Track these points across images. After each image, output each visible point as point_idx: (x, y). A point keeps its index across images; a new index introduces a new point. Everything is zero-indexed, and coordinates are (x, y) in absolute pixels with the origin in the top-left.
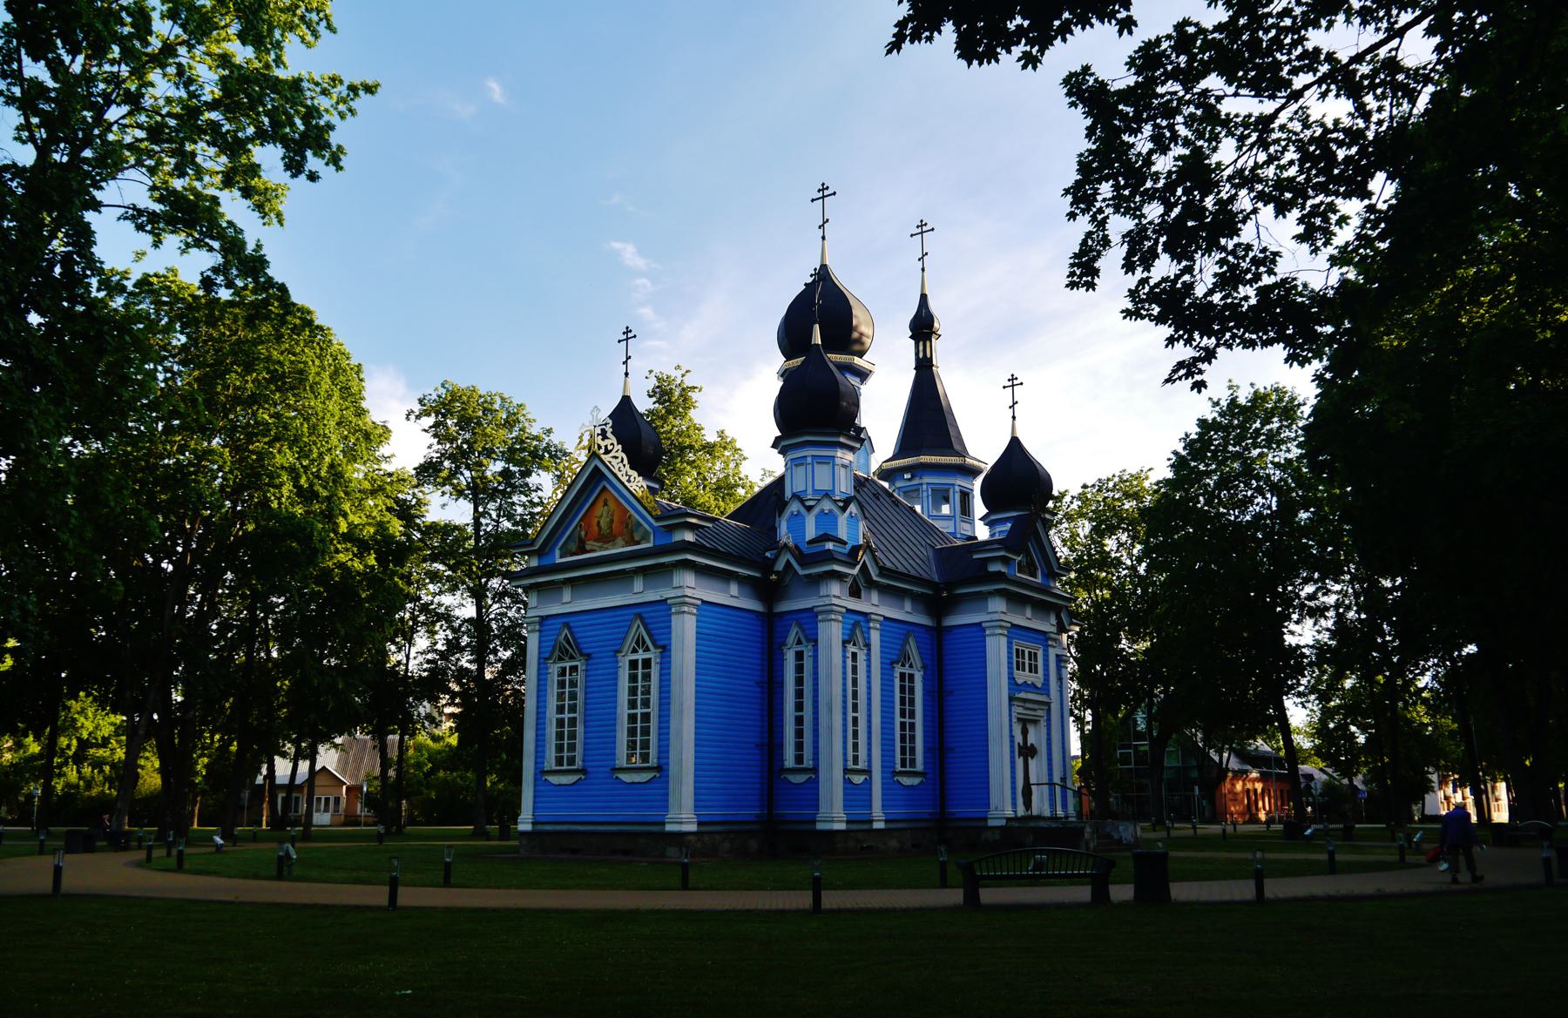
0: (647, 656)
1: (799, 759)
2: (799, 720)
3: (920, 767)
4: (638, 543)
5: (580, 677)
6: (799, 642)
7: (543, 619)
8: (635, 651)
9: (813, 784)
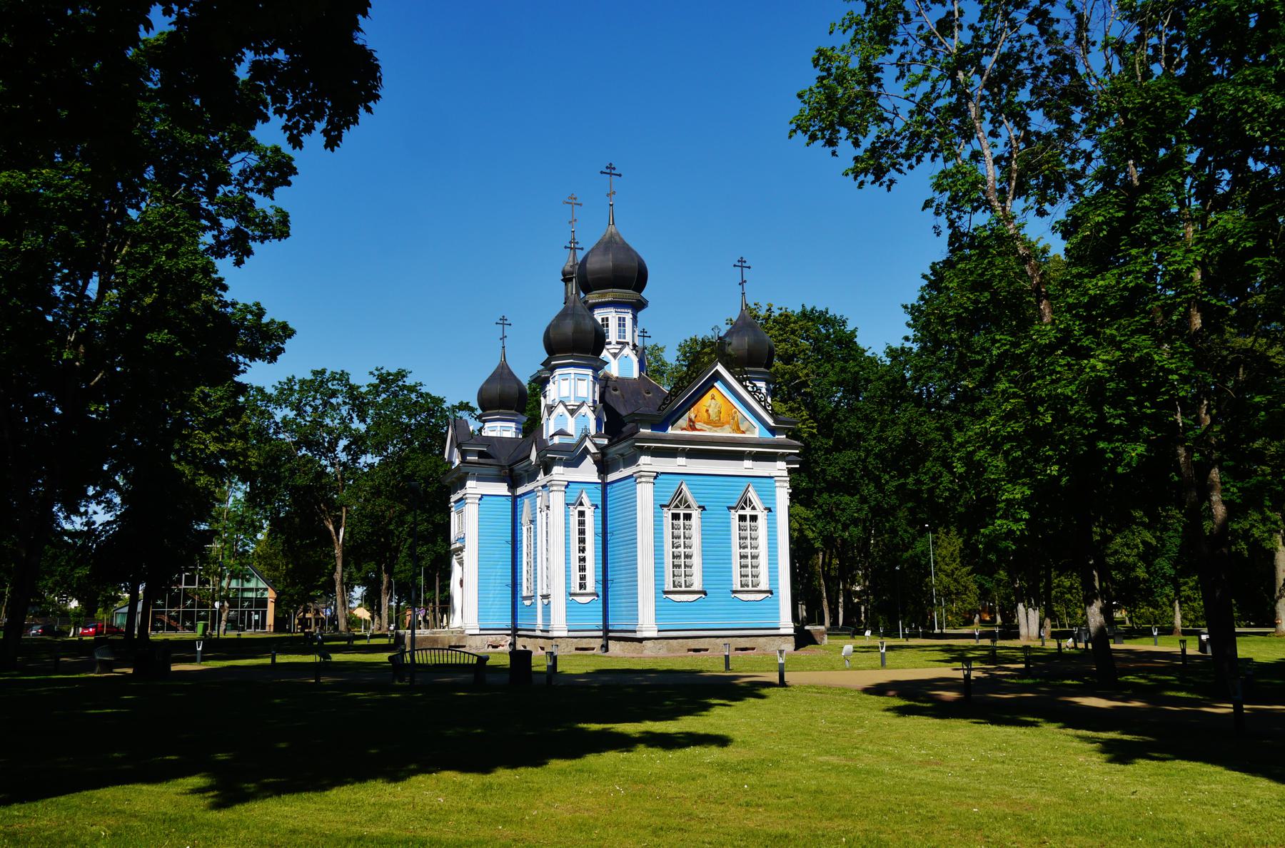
0: (753, 513)
7: (657, 475)
8: (743, 508)
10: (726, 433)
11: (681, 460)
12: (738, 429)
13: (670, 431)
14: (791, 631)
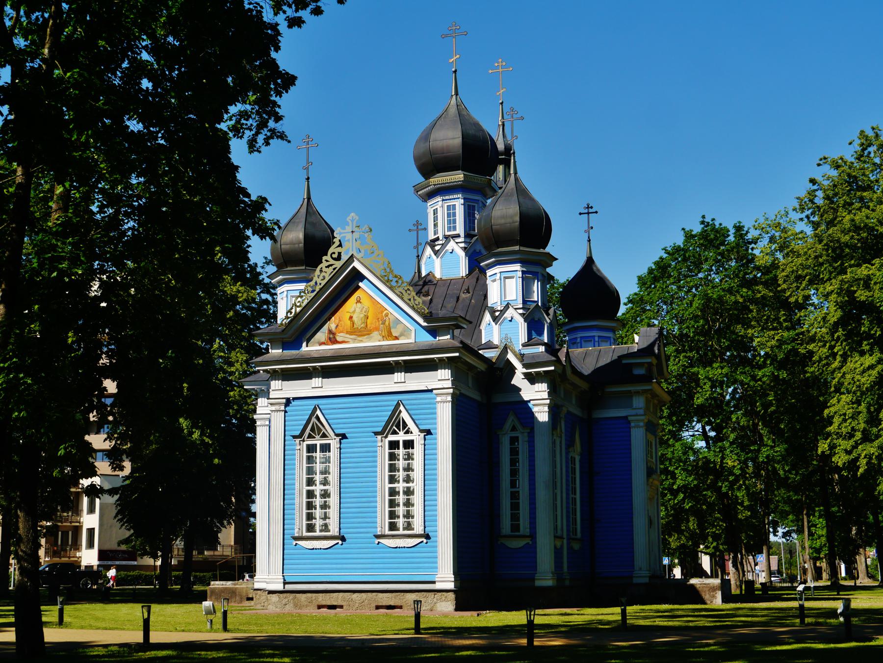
0: (408, 437)
1: (515, 527)
2: (515, 496)
3: (579, 535)
4: (397, 338)
5: (334, 454)
6: (514, 429)
7: (288, 402)
8: (395, 433)
9: (531, 549)
10: (374, 342)
11: (317, 381)
12: (389, 335)
13: (304, 348)
14: (451, 586)
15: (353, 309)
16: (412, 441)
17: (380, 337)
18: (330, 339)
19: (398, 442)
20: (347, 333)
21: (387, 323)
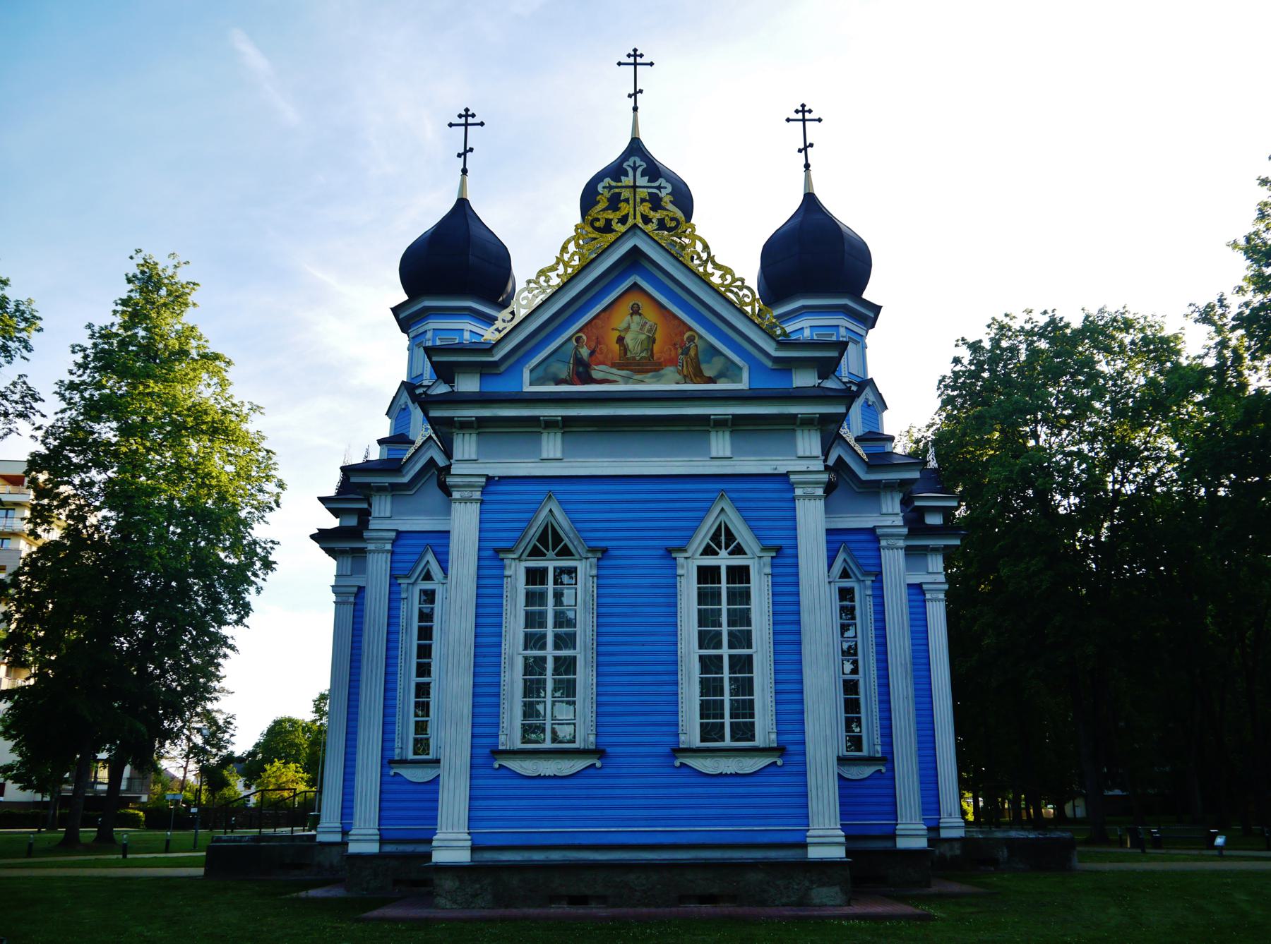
0: (738, 561)
4: (711, 380)
8: (708, 551)
12: (698, 376)
15: (624, 325)
16: (747, 568)
17: (678, 377)
18: (578, 374)
19: (718, 568)
20: (613, 365)
21: (692, 353)
